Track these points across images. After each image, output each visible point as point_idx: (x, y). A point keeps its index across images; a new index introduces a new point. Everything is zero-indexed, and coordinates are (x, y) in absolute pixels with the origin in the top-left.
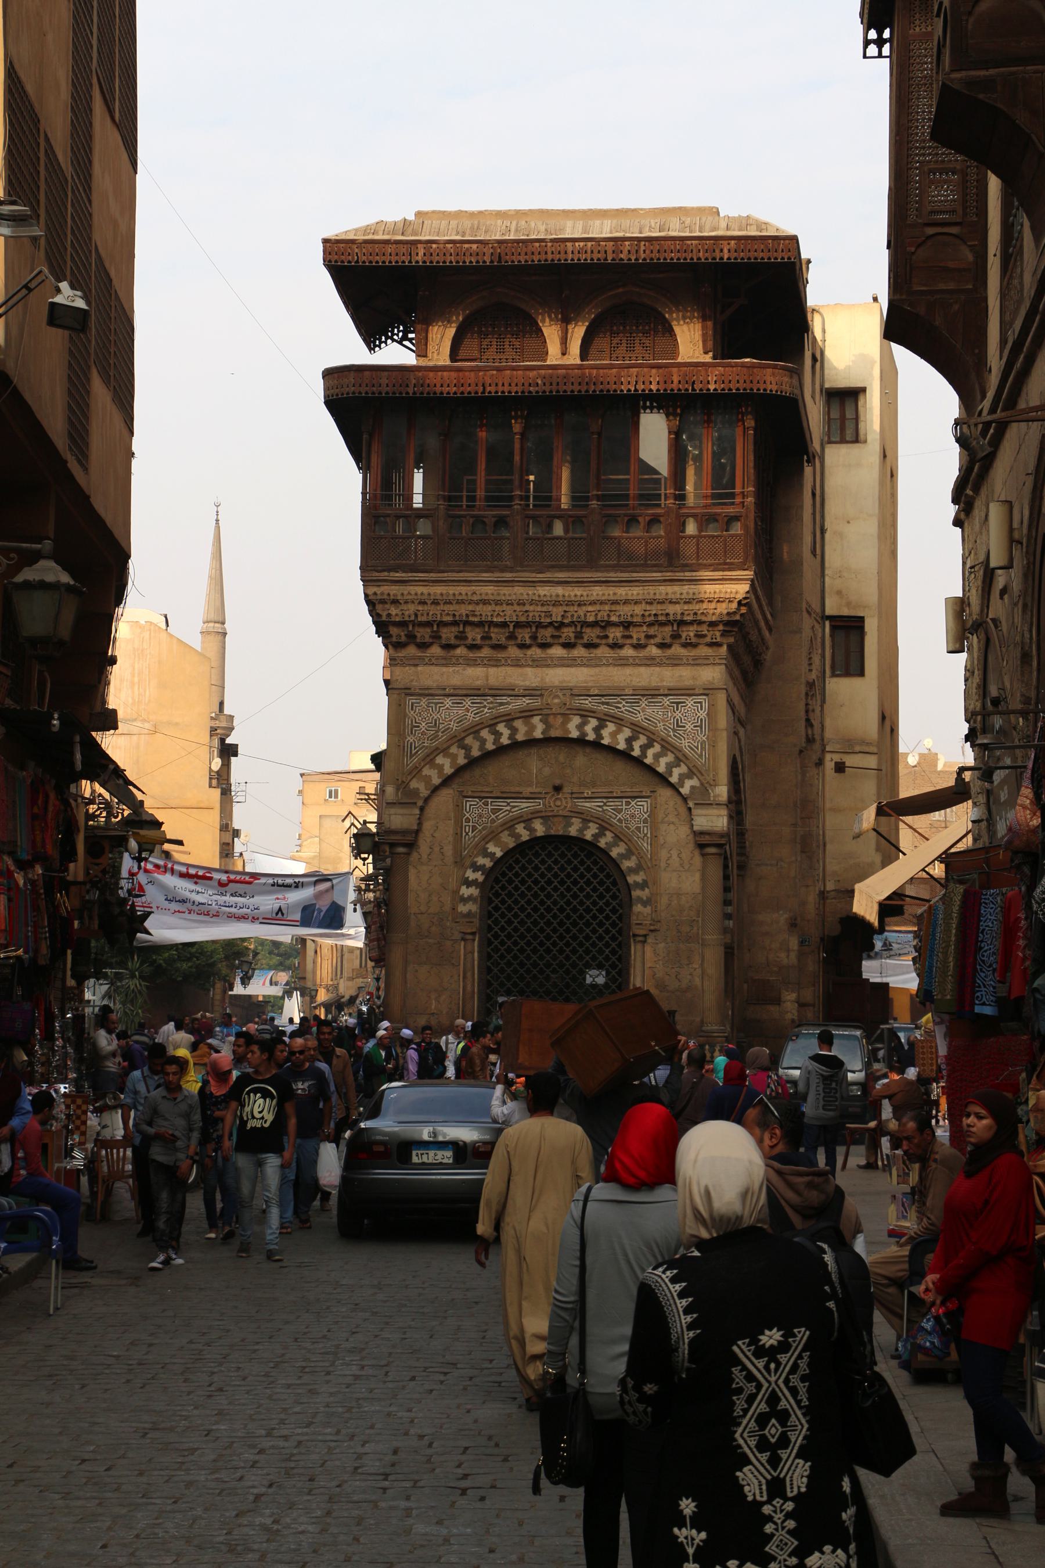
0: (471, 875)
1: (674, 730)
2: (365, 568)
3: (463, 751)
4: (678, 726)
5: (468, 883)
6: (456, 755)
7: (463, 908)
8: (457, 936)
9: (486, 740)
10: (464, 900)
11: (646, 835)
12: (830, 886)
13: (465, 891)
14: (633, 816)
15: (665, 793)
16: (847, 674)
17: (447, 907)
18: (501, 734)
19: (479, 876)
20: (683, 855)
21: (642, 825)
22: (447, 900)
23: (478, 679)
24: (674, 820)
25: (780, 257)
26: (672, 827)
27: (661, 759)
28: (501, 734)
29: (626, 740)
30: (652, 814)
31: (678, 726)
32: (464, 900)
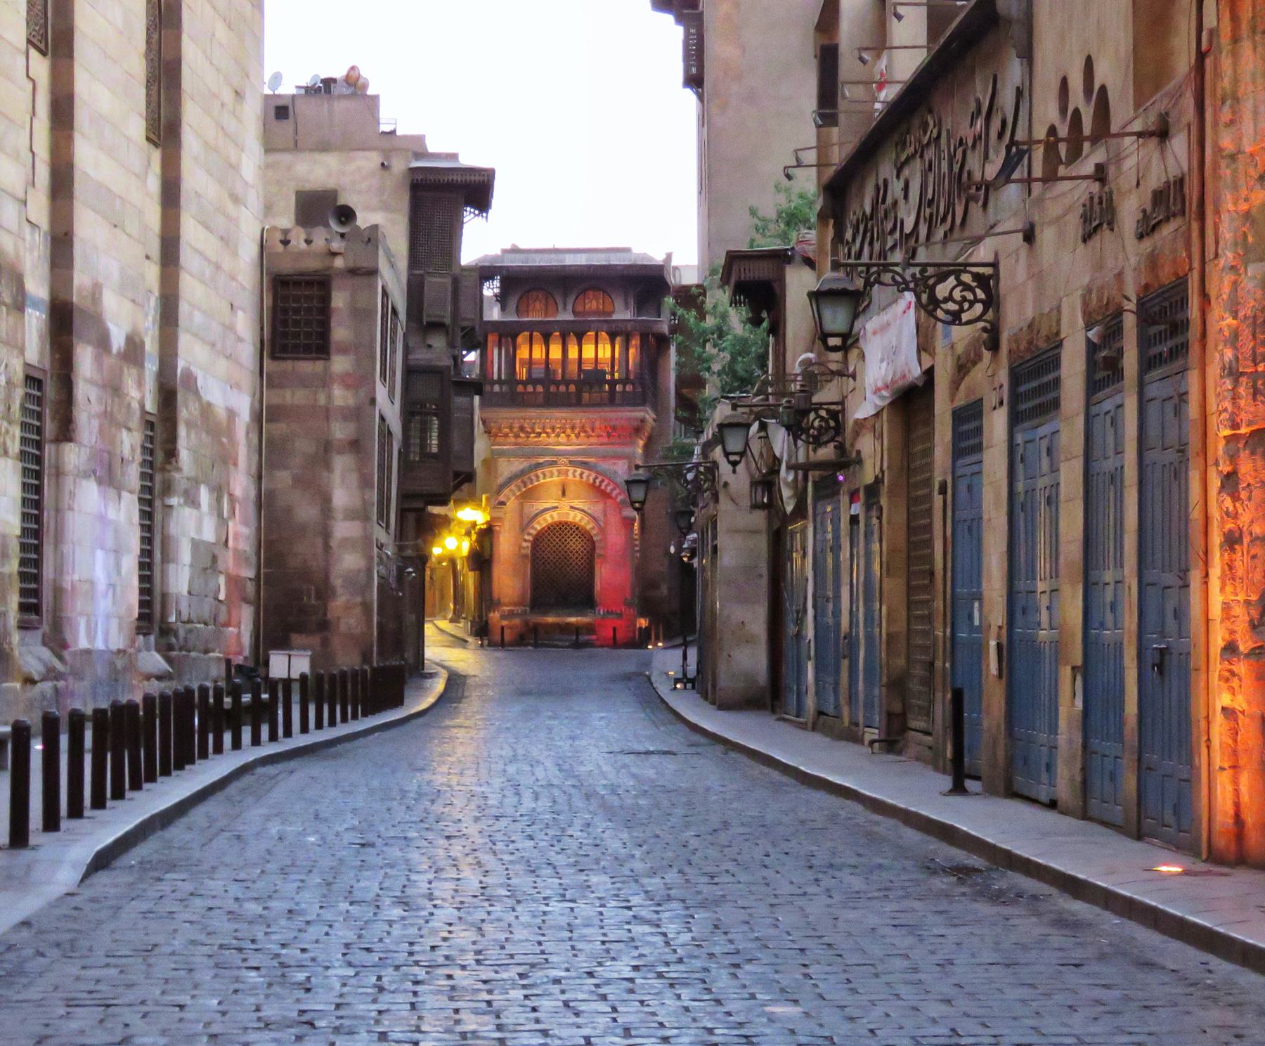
0: (527, 537)
7: (523, 551)
13: (525, 544)
15: (609, 502)
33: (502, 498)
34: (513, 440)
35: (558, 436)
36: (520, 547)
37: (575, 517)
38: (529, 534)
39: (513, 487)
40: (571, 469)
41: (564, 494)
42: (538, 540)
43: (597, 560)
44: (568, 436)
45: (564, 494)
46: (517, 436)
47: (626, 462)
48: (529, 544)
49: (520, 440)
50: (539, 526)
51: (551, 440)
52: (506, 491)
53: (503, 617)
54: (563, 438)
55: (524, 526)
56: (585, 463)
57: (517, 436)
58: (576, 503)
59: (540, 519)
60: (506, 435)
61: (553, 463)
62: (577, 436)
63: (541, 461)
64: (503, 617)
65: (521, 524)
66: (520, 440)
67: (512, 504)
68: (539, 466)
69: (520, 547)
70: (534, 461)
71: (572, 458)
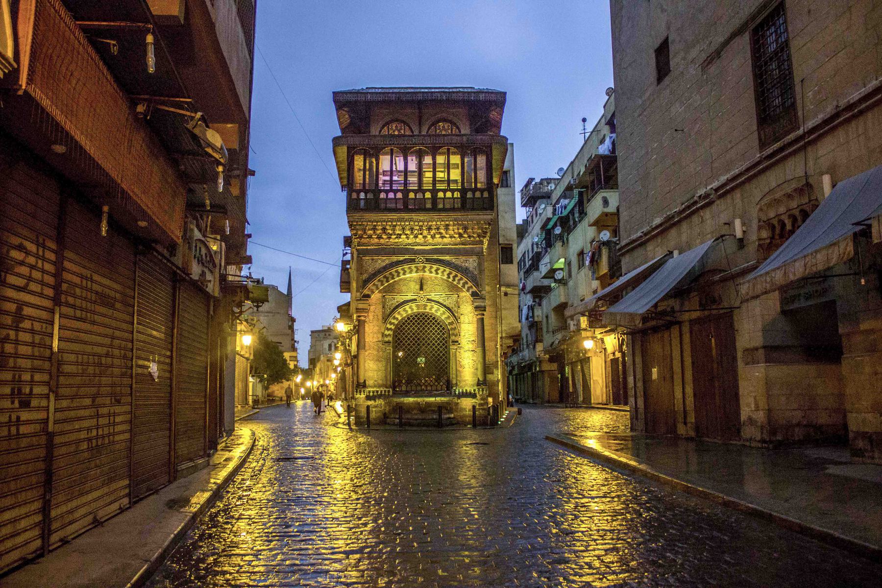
0: (389, 326)
5: (388, 329)
7: (386, 339)
10: (387, 336)
12: (504, 335)
13: (387, 332)
16: (507, 263)
19: (393, 327)
22: (380, 336)
32: (387, 336)
33: (366, 292)
35: (416, 237)
36: (383, 335)
38: (391, 323)
39: (376, 282)
40: (428, 266)
41: (421, 289)
42: (400, 329)
44: (425, 237)
45: (421, 289)
47: (475, 258)
50: (401, 314)
51: (410, 241)
52: (370, 285)
53: (368, 398)
54: (420, 239)
55: (386, 318)
57: (379, 237)
58: (433, 296)
59: (401, 310)
60: (370, 237)
61: (413, 261)
62: (433, 237)
63: (402, 258)
64: (368, 398)
67: (376, 296)
68: (398, 263)
70: (395, 258)
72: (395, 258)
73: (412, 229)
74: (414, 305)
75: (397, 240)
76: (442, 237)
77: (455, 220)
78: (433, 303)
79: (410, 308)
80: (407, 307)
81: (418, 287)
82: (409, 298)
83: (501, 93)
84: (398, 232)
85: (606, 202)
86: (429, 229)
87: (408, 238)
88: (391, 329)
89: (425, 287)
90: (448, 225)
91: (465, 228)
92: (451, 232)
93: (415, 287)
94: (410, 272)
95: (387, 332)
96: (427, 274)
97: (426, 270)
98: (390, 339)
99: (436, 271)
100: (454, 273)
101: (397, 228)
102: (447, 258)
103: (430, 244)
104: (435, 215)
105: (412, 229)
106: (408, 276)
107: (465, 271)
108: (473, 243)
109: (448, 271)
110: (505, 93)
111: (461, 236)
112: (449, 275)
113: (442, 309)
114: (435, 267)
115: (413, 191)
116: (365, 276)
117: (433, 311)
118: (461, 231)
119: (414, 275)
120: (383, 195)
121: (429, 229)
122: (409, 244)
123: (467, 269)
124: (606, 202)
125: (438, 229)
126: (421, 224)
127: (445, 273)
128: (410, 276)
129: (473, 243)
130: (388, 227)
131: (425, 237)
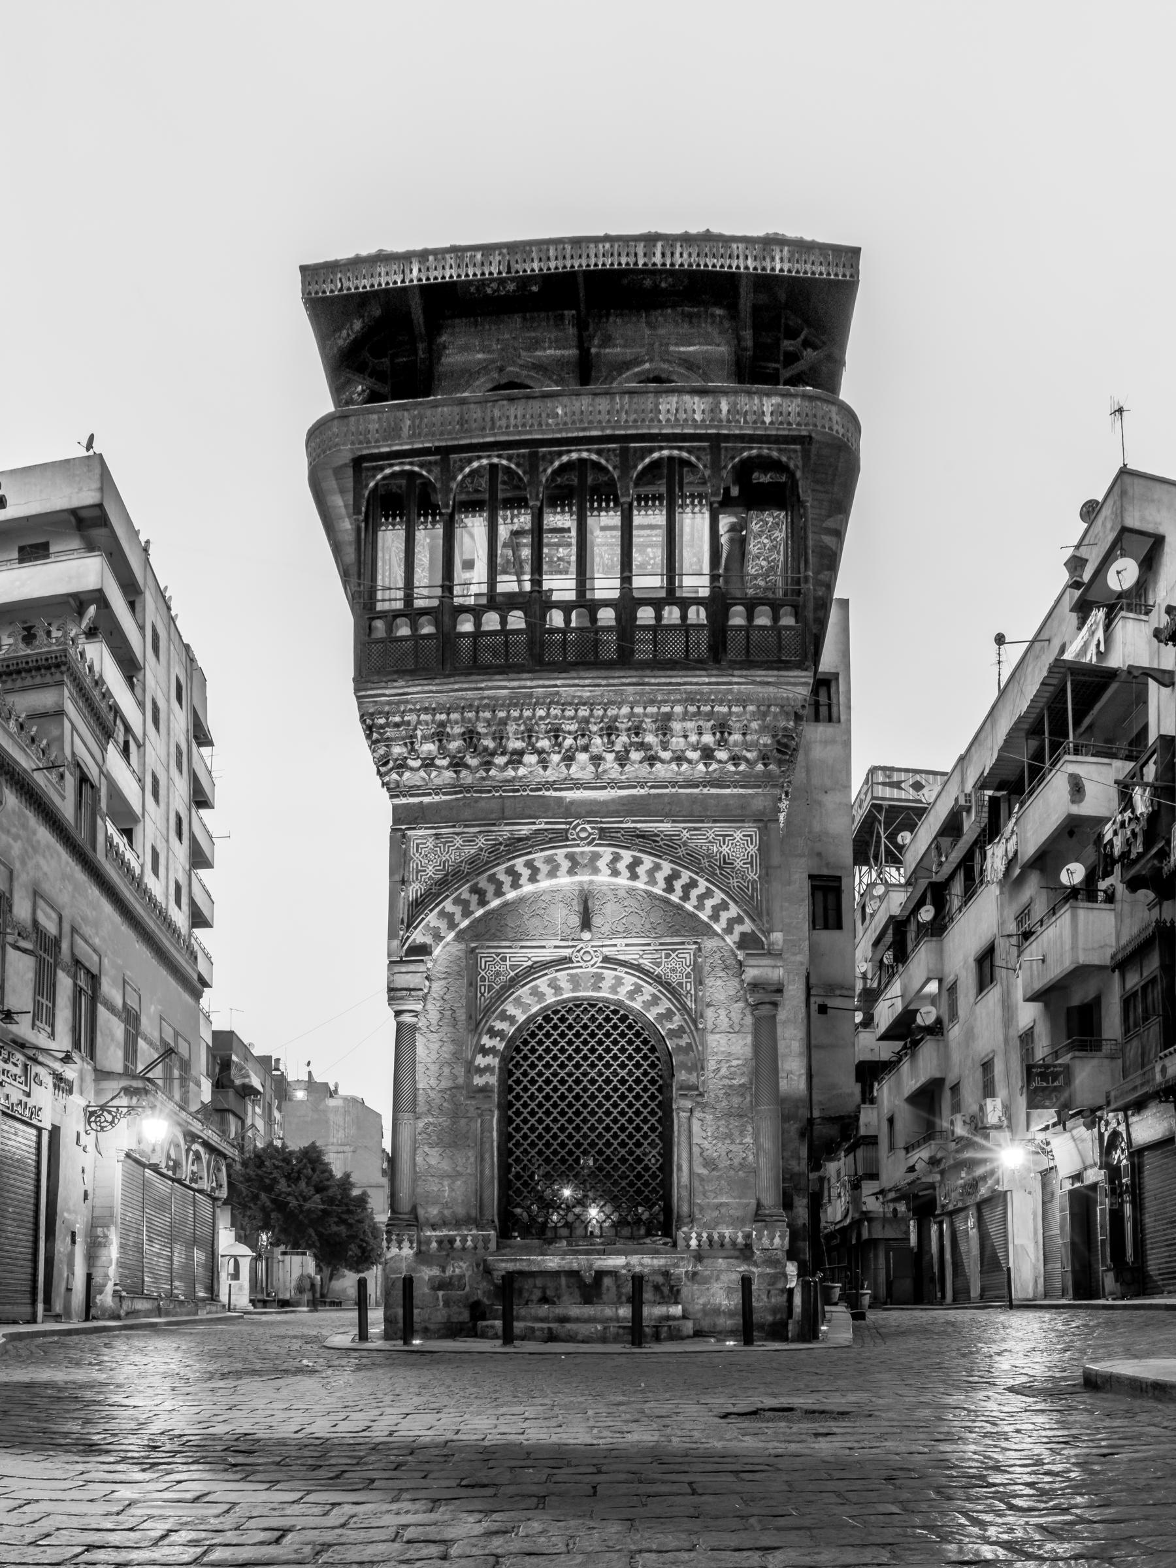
0: (487, 1041)
1: (721, 868)
2: (355, 681)
3: (477, 896)
4: (725, 863)
5: (485, 1051)
6: (469, 901)
7: (478, 1081)
8: (472, 1112)
9: (502, 883)
10: (481, 1071)
11: (688, 992)
13: (481, 1061)
14: (673, 970)
17: (461, 1081)
18: (520, 875)
20: (733, 1015)
21: (684, 980)
22: (460, 1071)
23: (492, 812)
24: (721, 974)
25: (838, 273)
26: (719, 982)
27: (706, 902)
28: (520, 875)
29: (665, 879)
30: (697, 968)
31: (725, 863)
32: (481, 1071)
33: (418, 936)
34: (449, 775)
35: (569, 759)
37: (620, 989)
38: (493, 1033)
39: (448, 906)
40: (607, 853)
41: (586, 924)
42: (518, 1052)
43: (681, 1104)
44: (597, 760)
45: (586, 924)
46: (457, 765)
48: (493, 1061)
49: (466, 777)
50: (522, 1007)
51: (551, 775)
52: (432, 919)
54: (582, 767)
56: (643, 836)
58: (623, 949)
59: (524, 992)
60: (429, 764)
61: (561, 838)
62: (622, 759)
63: (525, 830)
65: (472, 1002)
66: (466, 777)
68: (517, 845)
69: (472, 1069)
70: (505, 831)
71: (610, 823)
72: (505, 831)
73: (556, 733)
74: (562, 977)
75: (510, 773)
76: (652, 760)
77: (690, 699)
78: (621, 972)
79: (554, 986)
80: (542, 984)
81: (575, 920)
82: (547, 954)
83: (838, 250)
84: (515, 744)
85: (1077, 789)
86: (610, 731)
87: (544, 763)
88: (493, 1051)
89: (596, 921)
90: (668, 717)
91: (722, 728)
92: (677, 742)
93: (566, 917)
94: (552, 874)
95: (481, 1061)
96: (603, 878)
97: (602, 864)
98: (493, 1080)
99: (633, 867)
100: (686, 875)
101: (511, 728)
102: (666, 827)
103: (614, 784)
104: (626, 684)
105: (556, 733)
106: (544, 884)
107: (719, 870)
108: (744, 781)
109: (667, 868)
110: (856, 252)
111: (707, 754)
112: (670, 880)
113: (649, 990)
114: (627, 856)
115: (560, 605)
116: (414, 890)
117: (622, 994)
118: (708, 739)
119: (564, 881)
120: (466, 626)
121: (610, 731)
122: (549, 785)
123: (726, 862)
124: (1077, 789)
125: (637, 730)
126: (583, 712)
127: (660, 876)
128: (547, 884)
129: (744, 781)
130: (481, 729)
131: (597, 760)
